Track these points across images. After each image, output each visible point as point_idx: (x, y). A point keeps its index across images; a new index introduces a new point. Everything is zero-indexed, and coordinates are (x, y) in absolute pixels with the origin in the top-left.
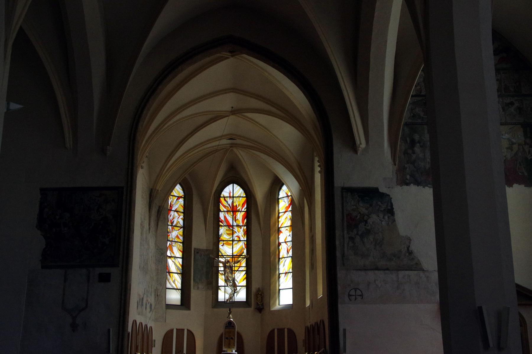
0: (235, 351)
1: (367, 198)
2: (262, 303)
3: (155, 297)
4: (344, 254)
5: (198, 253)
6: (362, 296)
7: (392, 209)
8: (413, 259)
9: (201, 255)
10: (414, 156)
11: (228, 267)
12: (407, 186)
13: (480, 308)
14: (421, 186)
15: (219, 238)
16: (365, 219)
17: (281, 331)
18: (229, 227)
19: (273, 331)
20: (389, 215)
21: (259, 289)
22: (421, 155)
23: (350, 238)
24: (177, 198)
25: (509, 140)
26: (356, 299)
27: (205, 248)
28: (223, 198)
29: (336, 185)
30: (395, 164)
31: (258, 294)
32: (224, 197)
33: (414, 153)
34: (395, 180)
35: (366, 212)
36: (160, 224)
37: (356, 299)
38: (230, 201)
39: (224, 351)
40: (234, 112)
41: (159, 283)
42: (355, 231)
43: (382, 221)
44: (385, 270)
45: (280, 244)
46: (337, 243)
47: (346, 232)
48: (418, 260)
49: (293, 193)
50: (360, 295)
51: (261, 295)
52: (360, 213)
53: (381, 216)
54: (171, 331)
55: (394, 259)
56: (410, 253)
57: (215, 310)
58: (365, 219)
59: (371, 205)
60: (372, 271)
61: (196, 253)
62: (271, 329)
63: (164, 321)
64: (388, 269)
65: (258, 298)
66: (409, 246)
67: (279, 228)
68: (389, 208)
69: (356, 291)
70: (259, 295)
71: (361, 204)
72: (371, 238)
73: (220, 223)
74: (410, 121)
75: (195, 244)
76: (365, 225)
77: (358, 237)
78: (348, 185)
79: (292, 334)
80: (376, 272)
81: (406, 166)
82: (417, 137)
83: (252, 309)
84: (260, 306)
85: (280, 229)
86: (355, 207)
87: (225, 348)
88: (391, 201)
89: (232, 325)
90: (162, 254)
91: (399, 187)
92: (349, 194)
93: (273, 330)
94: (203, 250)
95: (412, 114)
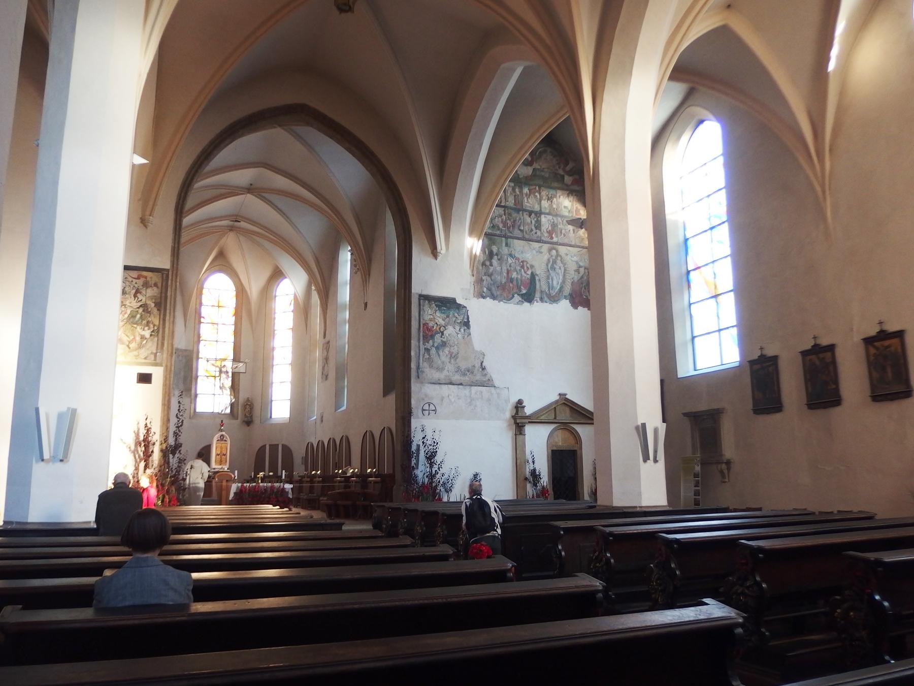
1: (444, 308)
4: (419, 366)
6: (435, 410)
7: (468, 321)
8: (486, 375)
10: (491, 269)
12: (484, 298)
13: (644, 425)
14: (497, 300)
16: (442, 330)
17: (274, 448)
19: (263, 448)
20: (466, 328)
21: (248, 398)
22: (498, 269)
23: (425, 348)
25: (577, 263)
26: (429, 414)
27: (183, 348)
28: (208, 290)
29: (413, 291)
30: (473, 275)
33: (491, 265)
34: (472, 291)
35: (443, 323)
37: (429, 414)
39: (214, 469)
40: (250, 189)
42: (431, 342)
43: (458, 334)
44: (459, 385)
46: (413, 353)
47: (421, 343)
48: (491, 376)
49: (298, 291)
50: (434, 410)
52: (436, 323)
53: (458, 328)
55: (468, 374)
56: (484, 369)
57: (194, 421)
58: (442, 330)
59: (448, 316)
60: (447, 385)
62: (261, 444)
64: (461, 384)
65: (246, 409)
66: (483, 362)
68: (466, 321)
69: (429, 405)
70: (248, 406)
71: (438, 314)
72: (447, 350)
73: (202, 320)
74: (490, 231)
76: (442, 337)
77: (434, 349)
78: (424, 293)
79: (287, 451)
80: (450, 386)
81: (484, 278)
82: (495, 249)
83: (238, 421)
84: (249, 418)
86: (432, 317)
87: (216, 465)
88: (467, 313)
89: (225, 439)
91: (475, 299)
92: (427, 302)
95: (492, 225)
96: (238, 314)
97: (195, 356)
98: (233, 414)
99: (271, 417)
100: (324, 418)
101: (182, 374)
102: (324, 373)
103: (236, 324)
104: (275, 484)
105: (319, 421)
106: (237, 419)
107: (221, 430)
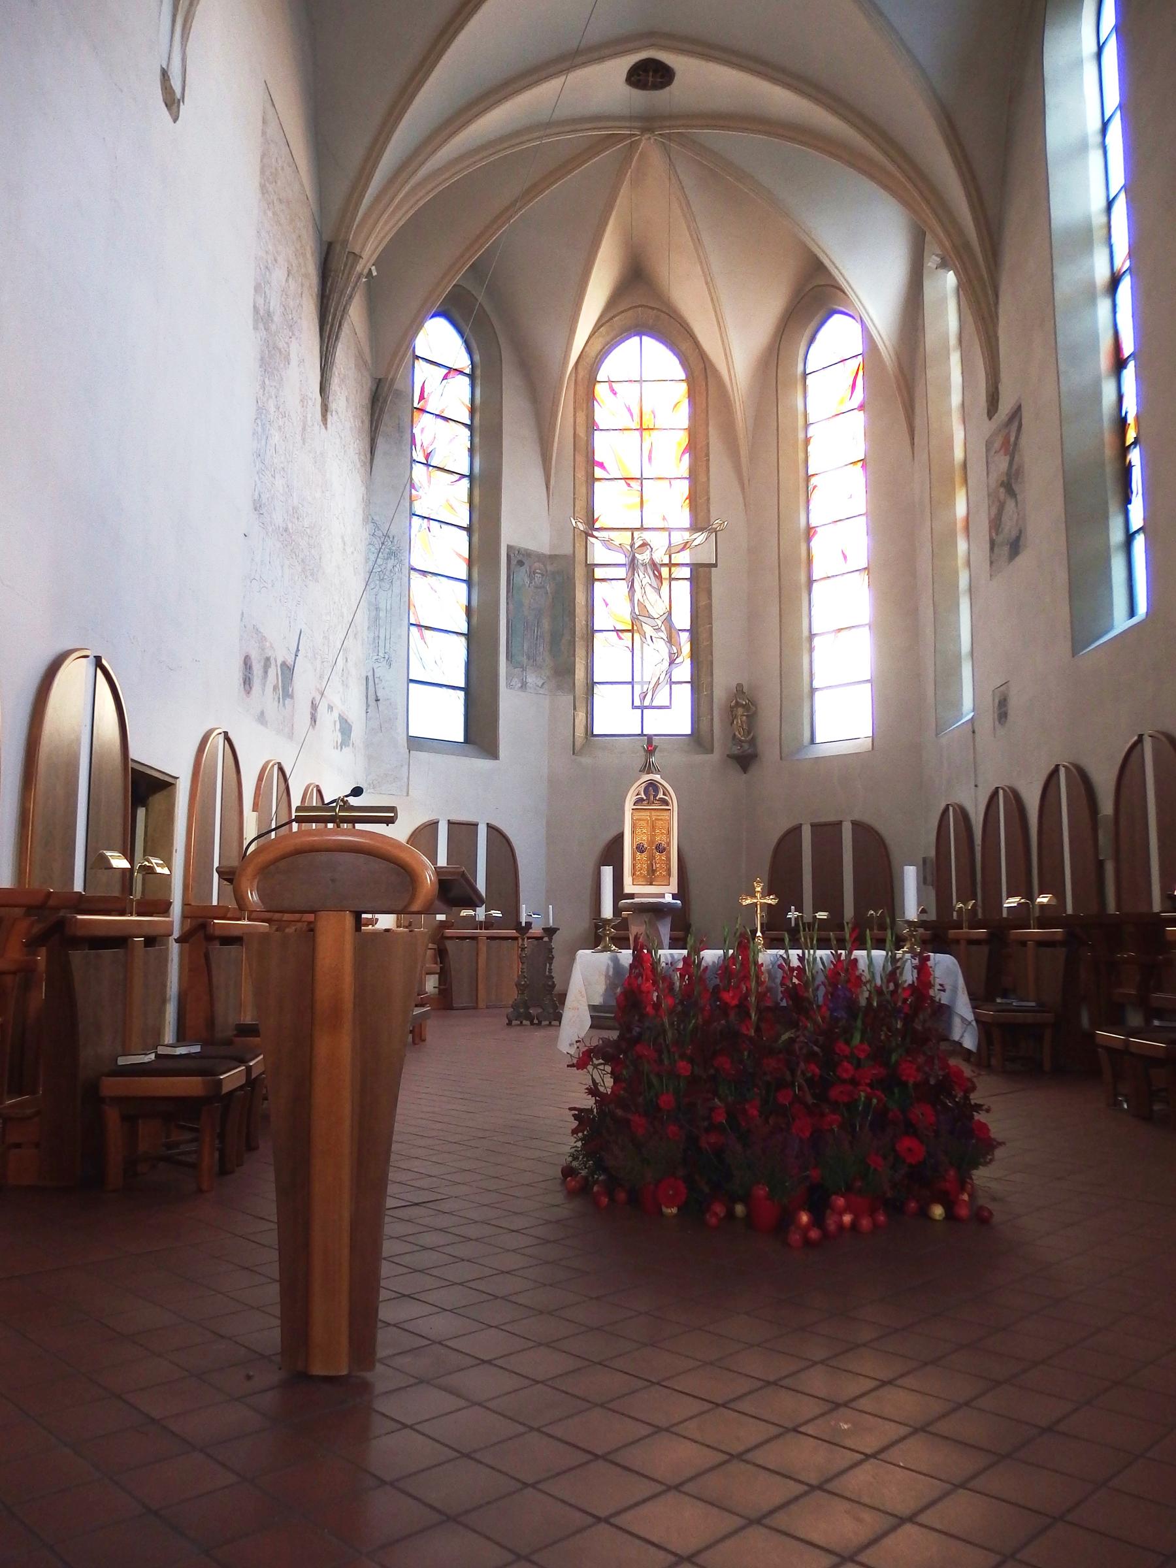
0: (674, 897)
2: (750, 737)
3: (368, 706)
5: (520, 563)
9: (534, 573)
11: (644, 565)
15: (594, 521)
17: (827, 833)
18: (628, 481)
19: (795, 832)
21: (739, 687)
24: (445, 371)
27: (546, 550)
31: (738, 704)
32: (610, 382)
36: (381, 442)
38: (629, 393)
39: (632, 896)
41: (381, 654)
45: (810, 532)
51: (746, 707)
54: (435, 824)
57: (586, 760)
61: (514, 562)
62: (785, 825)
63: (405, 794)
67: (808, 478)
70: (740, 711)
73: (598, 473)
75: (511, 533)
83: (716, 756)
84: (746, 746)
85: (813, 481)
89: (661, 795)
90: (393, 554)
93: (796, 830)
94: (541, 558)
96: (696, 448)
97: (580, 573)
98: (698, 739)
99: (812, 741)
100: (1014, 703)
101: (546, 624)
102: (999, 539)
103: (693, 477)
104: (859, 954)
105: (988, 721)
106: (712, 751)
107: (648, 768)
